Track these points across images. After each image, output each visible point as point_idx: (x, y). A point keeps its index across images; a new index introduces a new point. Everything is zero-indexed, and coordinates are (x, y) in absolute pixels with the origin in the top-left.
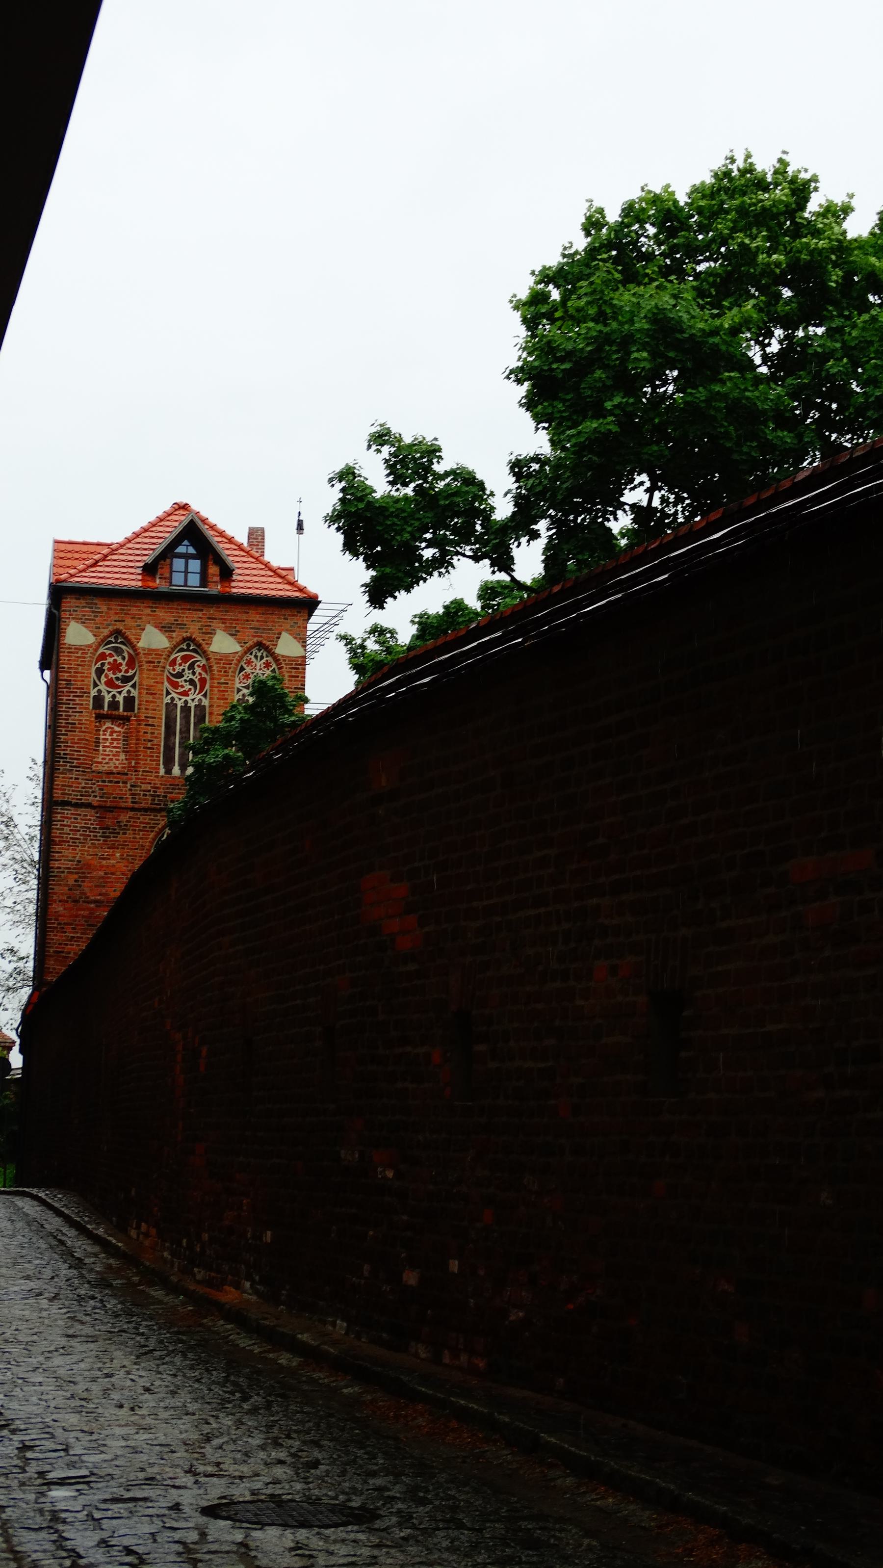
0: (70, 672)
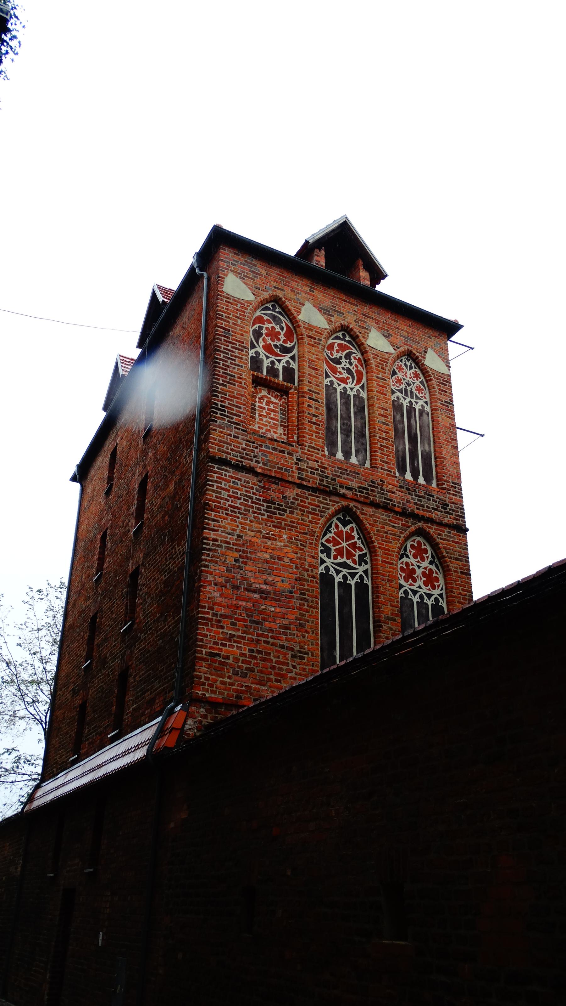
0: (229, 322)
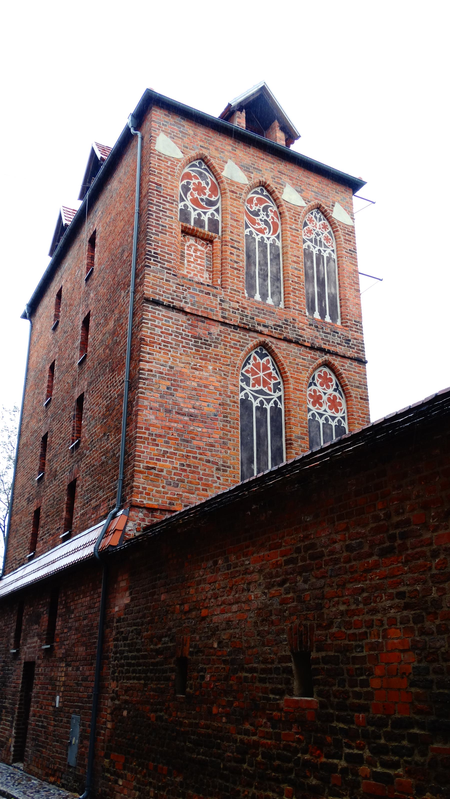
0: (161, 178)
